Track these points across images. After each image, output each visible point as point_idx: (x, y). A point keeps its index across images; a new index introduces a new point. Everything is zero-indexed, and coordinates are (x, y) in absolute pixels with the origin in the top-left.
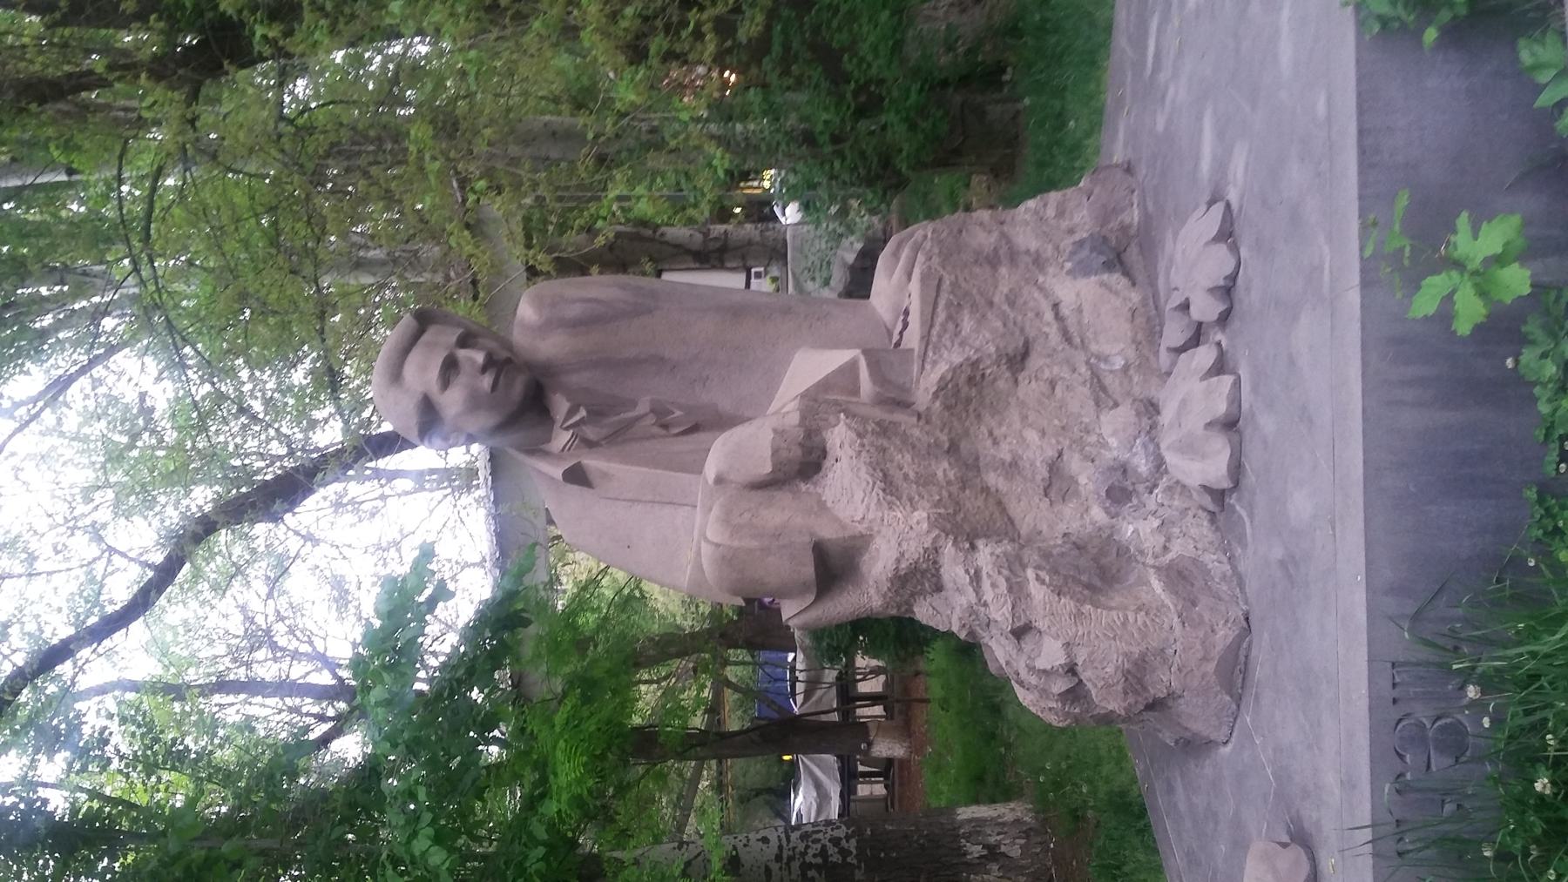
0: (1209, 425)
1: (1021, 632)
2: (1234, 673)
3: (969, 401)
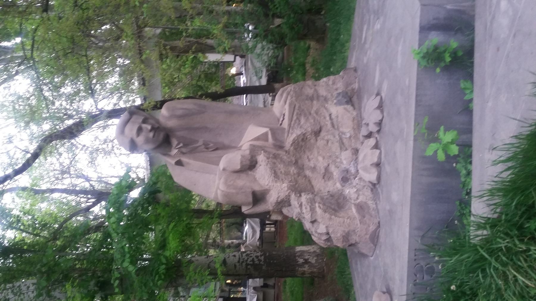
0: (372, 165)
2: (374, 238)
3: (302, 146)
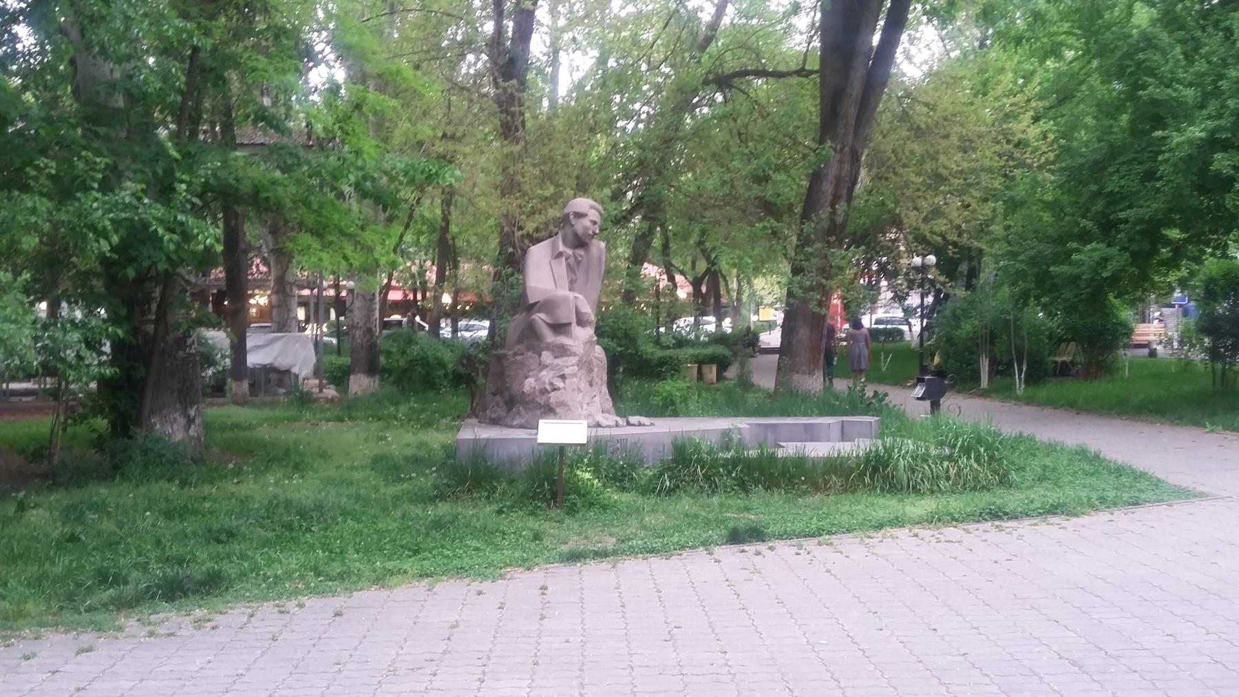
1: (563, 377)
